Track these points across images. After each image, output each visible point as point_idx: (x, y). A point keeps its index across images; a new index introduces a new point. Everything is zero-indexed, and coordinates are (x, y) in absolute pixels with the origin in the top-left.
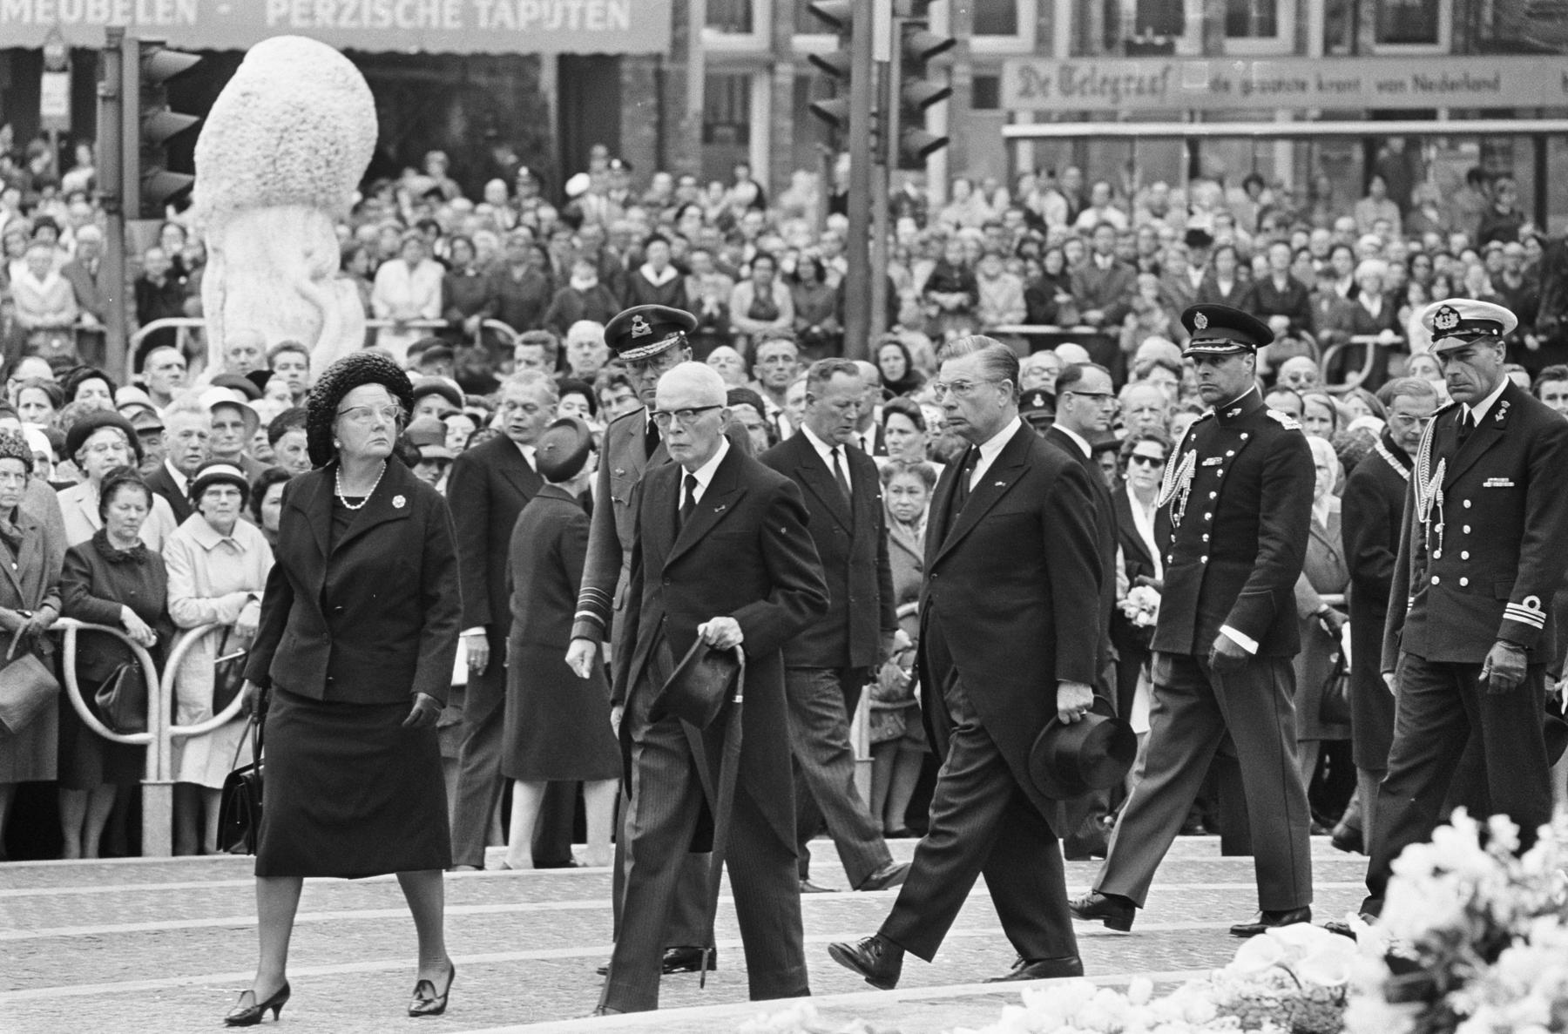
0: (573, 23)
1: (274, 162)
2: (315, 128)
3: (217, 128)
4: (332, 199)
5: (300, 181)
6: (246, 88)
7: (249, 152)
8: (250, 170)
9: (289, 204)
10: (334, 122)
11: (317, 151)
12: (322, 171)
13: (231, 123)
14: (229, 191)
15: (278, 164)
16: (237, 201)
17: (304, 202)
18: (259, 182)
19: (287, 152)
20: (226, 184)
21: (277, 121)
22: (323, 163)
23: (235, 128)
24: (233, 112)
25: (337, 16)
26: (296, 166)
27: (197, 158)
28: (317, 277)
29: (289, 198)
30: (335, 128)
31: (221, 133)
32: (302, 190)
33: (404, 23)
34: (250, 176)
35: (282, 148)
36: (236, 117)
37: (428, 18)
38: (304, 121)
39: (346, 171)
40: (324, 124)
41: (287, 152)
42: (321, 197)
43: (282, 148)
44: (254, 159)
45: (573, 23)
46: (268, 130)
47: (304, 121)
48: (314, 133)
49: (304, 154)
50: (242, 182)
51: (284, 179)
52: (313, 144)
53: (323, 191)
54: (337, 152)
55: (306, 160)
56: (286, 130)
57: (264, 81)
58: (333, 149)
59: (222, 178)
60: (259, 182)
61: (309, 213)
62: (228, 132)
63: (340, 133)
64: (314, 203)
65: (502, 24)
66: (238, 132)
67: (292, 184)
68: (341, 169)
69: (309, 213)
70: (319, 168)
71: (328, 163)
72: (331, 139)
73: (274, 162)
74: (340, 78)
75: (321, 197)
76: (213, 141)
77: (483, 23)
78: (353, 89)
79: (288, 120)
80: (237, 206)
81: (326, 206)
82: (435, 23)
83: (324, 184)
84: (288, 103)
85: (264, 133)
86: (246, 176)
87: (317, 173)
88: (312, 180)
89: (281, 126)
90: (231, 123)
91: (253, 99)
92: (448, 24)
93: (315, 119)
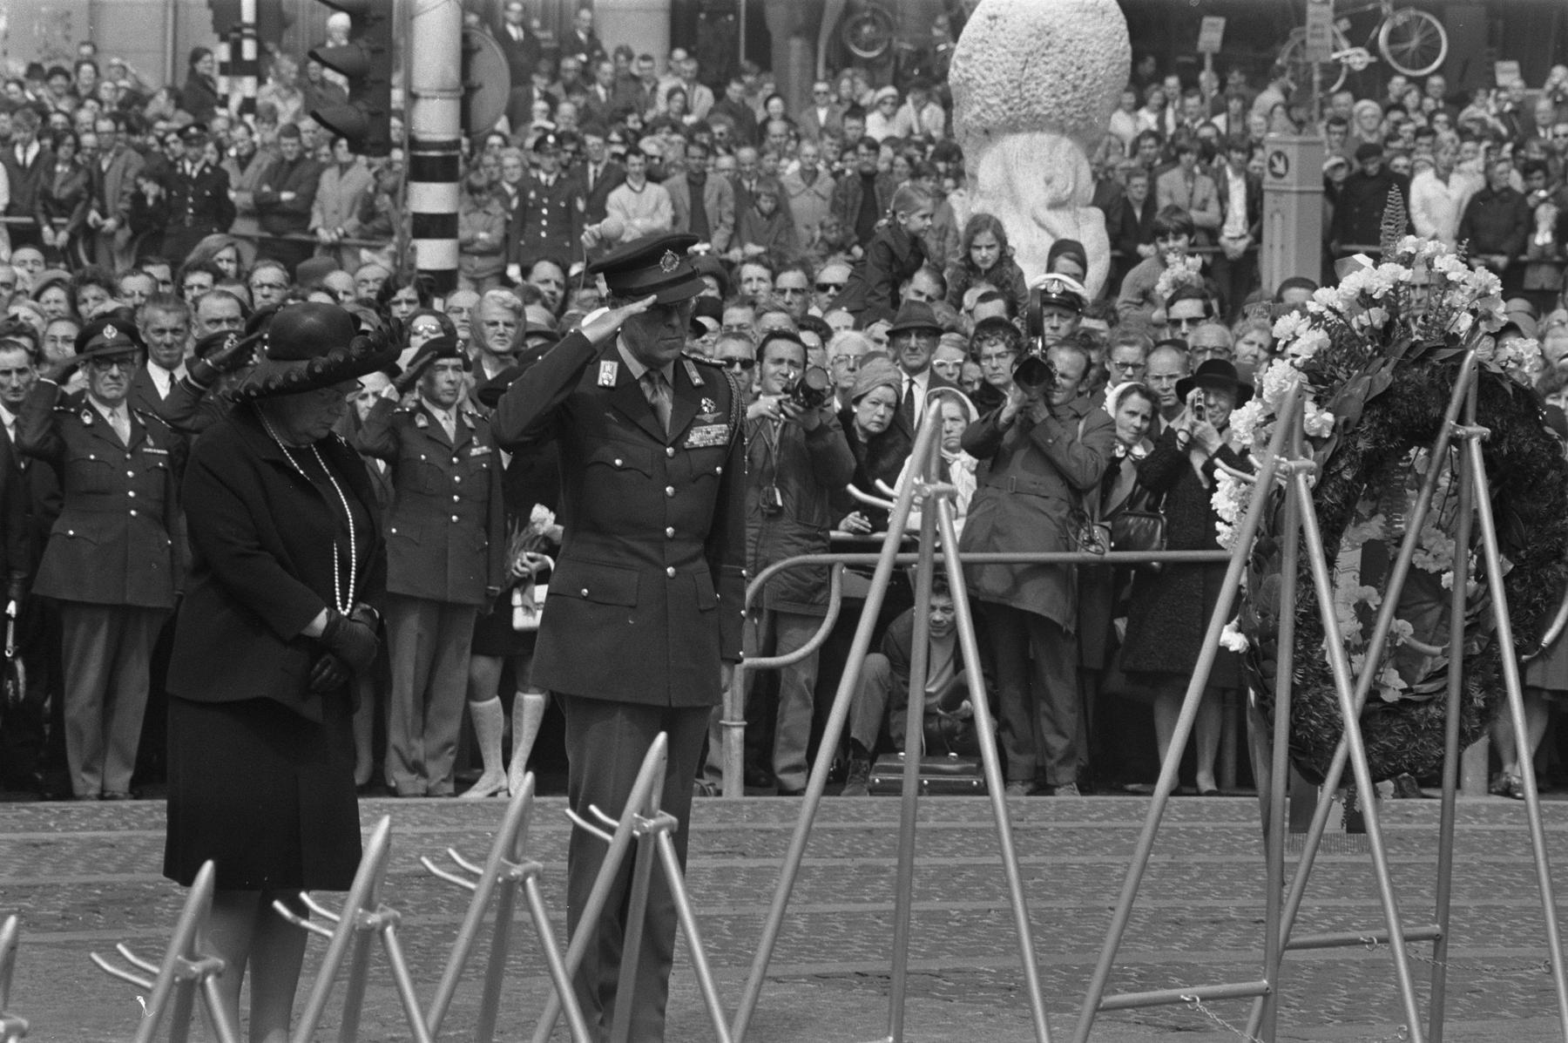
4: (1082, 125)
6: (992, 11)
11: (1063, 76)
12: (1068, 97)
13: (978, 46)
14: (978, 117)
18: (1005, 107)
22: (1069, 88)
29: (1036, 124)
32: (1049, 116)
38: (1049, 45)
40: (1071, 48)
46: (1014, 54)
47: (1049, 45)
48: (1060, 56)
49: (1049, 79)
50: (990, 106)
51: (1029, 104)
53: (1071, 116)
54: (1084, 76)
56: (1031, 53)
58: (1081, 73)
67: (1038, 109)
69: (1054, 145)
70: (1065, 93)
71: (1075, 88)
80: (987, 132)
83: (1069, 110)
89: (1027, 49)
91: (1000, 21)
93: (1060, 43)
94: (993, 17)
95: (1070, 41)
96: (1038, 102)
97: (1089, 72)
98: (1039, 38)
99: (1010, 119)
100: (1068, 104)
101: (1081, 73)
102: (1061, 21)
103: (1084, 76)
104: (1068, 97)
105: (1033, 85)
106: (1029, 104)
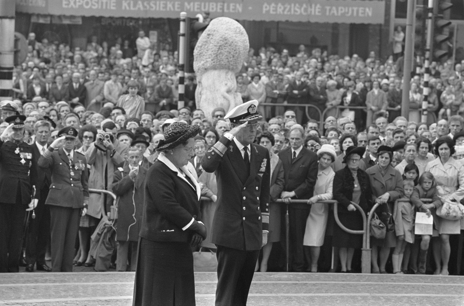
0: (355, 14)
1: (217, 56)
2: (230, 46)
3: (200, 45)
4: (235, 67)
5: (225, 62)
6: (209, 33)
7: (210, 52)
8: (209, 58)
9: (221, 69)
10: (235, 44)
11: (230, 53)
12: (232, 59)
13: (204, 43)
14: (203, 65)
15: (218, 57)
16: (206, 67)
17: (226, 68)
18: (212, 62)
19: (221, 53)
20: (202, 62)
21: (218, 43)
22: (232, 56)
23: (205, 45)
24: (205, 40)
25: (283, 11)
26: (223, 57)
27: (194, 54)
28: (229, 91)
30: (236, 45)
31: (201, 46)
32: (226, 65)
33: (304, 14)
34: (210, 60)
35: (219, 52)
36: (206, 42)
37: (311, 12)
38: (226, 43)
39: (239, 59)
41: (221, 53)
42: (231, 67)
43: (219, 52)
44: (211, 55)
45: (355, 14)
46: (215, 46)
47: (226, 43)
48: (229, 47)
49: (226, 54)
50: (207, 62)
51: (220, 61)
52: (229, 50)
54: (236, 53)
55: (226, 55)
56: (221, 46)
57: (214, 31)
58: (235, 52)
59: (202, 60)
60: (212, 62)
61: (227, 73)
62: (203, 46)
63: (237, 47)
64: (229, 69)
65: (333, 14)
66: (206, 47)
67: (223, 63)
68: (237, 58)
69: (227, 73)
70: (230, 58)
71: (233, 56)
72: (234, 49)
73: (217, 56)
74: (238, 30)
75: (231, 67)
76: (199, 49)
77: (328, 13)
78: (242, 34)
79: (222, 43)
80: (206, 69)
81: (232, 70)
82: (313, 13)
83: (232, 63)
84: (222, 37)
85: (214, 47)
86: (208, 60)
87: (230, 59)
88: (228, 61)
89: (219, 44)
90: (204, 43)
91: (211, 36)
92: (317, 13)
93: (230, 43)
94: (209, 35)
95: (232, 42)
96: (223, 61)
97: (238, 52)
98: (223, 41)
99: (214, 65)
100: (231, 61)
101: (235, 52)
102: (230, 36)
103: (236, 53)
104: (232, 59)
105: (221, 56)
106: (220, 61)
